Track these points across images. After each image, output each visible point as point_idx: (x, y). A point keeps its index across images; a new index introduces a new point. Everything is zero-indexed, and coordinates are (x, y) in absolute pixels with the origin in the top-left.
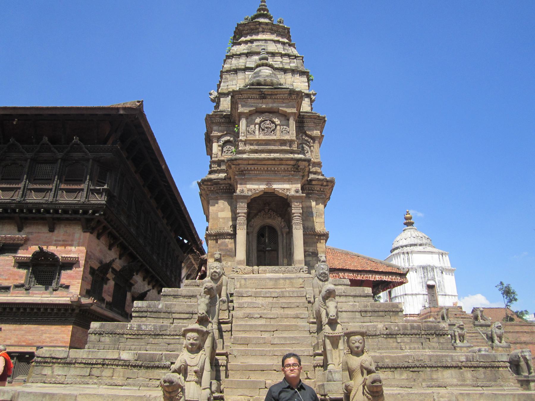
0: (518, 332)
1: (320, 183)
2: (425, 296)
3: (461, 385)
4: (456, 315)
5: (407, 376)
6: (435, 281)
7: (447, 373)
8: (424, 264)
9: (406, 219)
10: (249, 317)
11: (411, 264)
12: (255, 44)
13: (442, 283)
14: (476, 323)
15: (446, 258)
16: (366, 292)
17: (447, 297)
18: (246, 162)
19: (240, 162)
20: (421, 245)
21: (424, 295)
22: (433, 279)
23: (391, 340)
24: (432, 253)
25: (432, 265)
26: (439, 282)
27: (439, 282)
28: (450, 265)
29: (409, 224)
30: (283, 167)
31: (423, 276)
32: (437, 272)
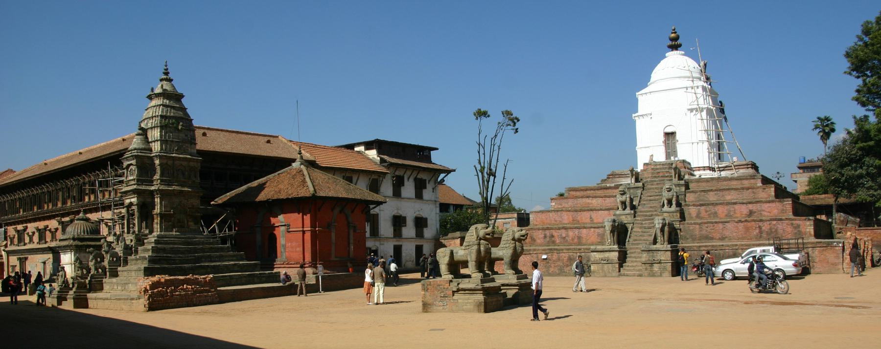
29: (675, 47)
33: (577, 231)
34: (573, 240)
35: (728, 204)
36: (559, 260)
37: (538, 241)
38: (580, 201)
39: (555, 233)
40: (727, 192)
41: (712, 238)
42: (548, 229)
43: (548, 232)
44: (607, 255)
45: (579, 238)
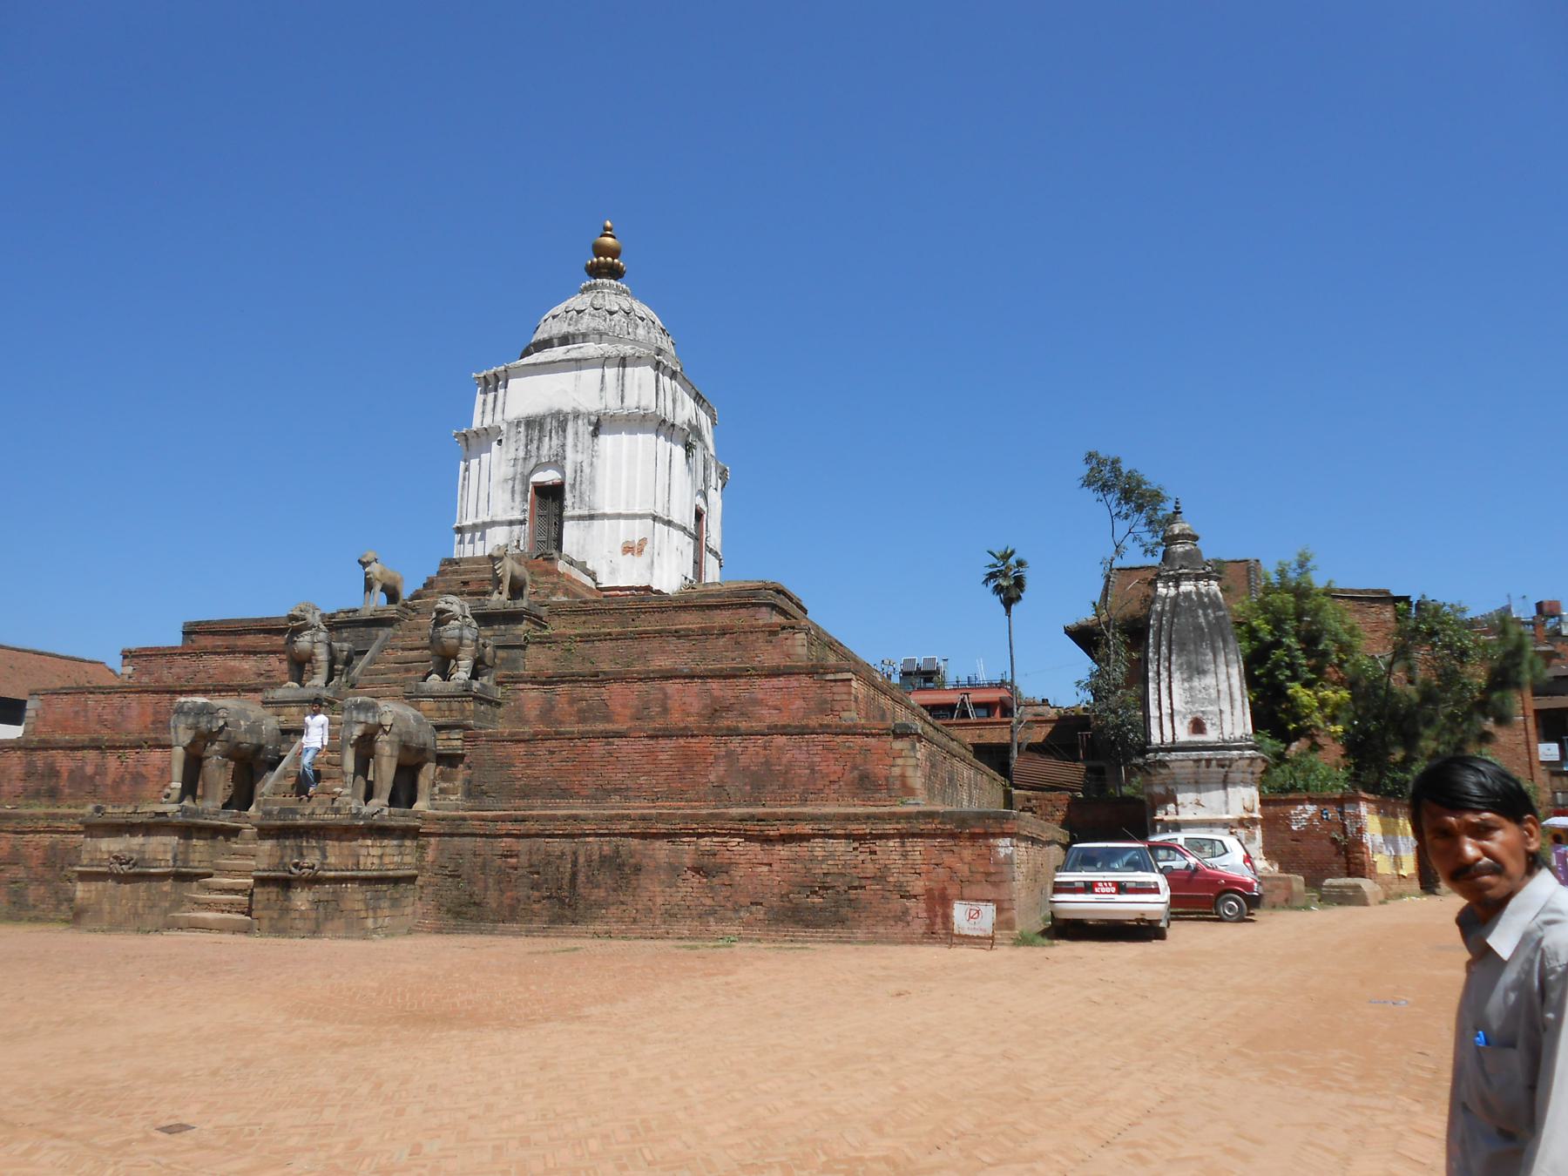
0: (641, 636)
2: (516, 528)
4: (465, 583)
6: (563, 473)
11: (498, 417)
13: (587, 470)
17: (595, 522)
20: (565, 340)
21: (511, 523)
22: (558, 463)
24: (579, 363)
25: (567, 408)
26: (579, 469)
27: (579, 469)
29: (605, 269)
31: (521, 454)
34: (117, 785)
35: (646, 678)
38: (214, 663)
39: (63, 761)
40: (655, 643)
41: (565, 794)
43: (39, 758)
44: (138, 840)
45: (138, 778)
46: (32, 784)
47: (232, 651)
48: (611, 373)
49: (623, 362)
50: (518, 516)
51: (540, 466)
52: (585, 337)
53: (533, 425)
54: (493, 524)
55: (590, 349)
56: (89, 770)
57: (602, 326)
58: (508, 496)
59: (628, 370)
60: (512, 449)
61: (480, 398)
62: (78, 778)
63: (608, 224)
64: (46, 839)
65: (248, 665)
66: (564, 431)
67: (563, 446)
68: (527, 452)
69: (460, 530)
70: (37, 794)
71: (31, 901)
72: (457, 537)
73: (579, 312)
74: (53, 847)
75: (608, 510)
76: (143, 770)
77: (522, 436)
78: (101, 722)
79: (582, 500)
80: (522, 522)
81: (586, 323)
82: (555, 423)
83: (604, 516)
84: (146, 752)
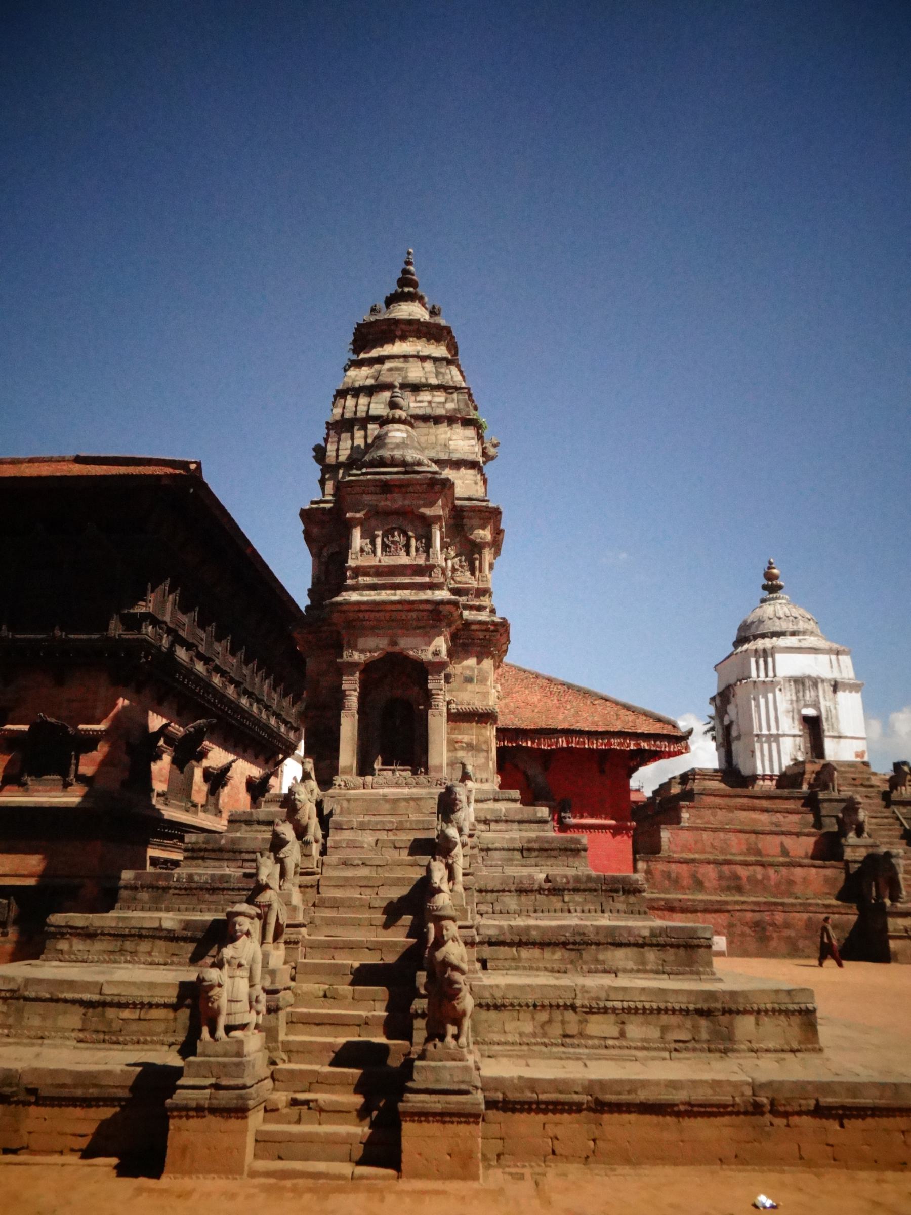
1: (484, 627)
2: (798, 739)
3: (638, 971)
4: (854, 779)
5: (563, 956)
7: (620, 953)
8: (797, 672)
9: (769, 576)
10: (346, 863)
11: (771, 674)
12: (388, 365)
13: (833, 711)
14: (895, 796)
15: (846, 660)
16: (539, 815)
17: (842, 740)
18: (356, 608)
19: (345, 608)
20: (793, 634)
21: (794, 736)
22: (816, 705)
23: (554, 899)
24: (815, 650)
26: (828, 710)
27: (828, 710)
28: (851, 675)
29: (772, 587)
30: (414, 614)
31: (794, 698)
32: (824, 691)
33: (784, 871)
34: (778, 885)
36: (787, 925)
37: (706, 884)
38: (743, 815)
42: (728, 862)
43: (725, 868)
45: (791, 883)
46: (724, 883)
47: (754, 809)
48: (833, 657)
49: (838, 653)
50: (797, 732)
51: (806, 706)
52: (804, 633)
53: (799, 682)
54: (784, 735)
55: (811, 641)
56: (759, 877)
57: (809, 627)
58: (791, 721)
59: (840, 657)
60: (788, 694)
61: (753, 660)
62: (751, 880)
63: (772, 561)
64: (805, 916)
65: (764, 817)
66: (817, 688)
67: (818, 696)
68: (797, 697)
69: (757, 735)
70: (729, 888)
71: (801, 946)
72: (756, 739)
73: (796, 618)
74: (810, 919)
75: (849, 735)
76: (791, 878)
77: (793, 687)
78: (713, 847)
79: (833, 728)
80: (800, 736)
81: (802, 625)
82: (811, 683)
83: (846, 737)
84: (792, 869)
